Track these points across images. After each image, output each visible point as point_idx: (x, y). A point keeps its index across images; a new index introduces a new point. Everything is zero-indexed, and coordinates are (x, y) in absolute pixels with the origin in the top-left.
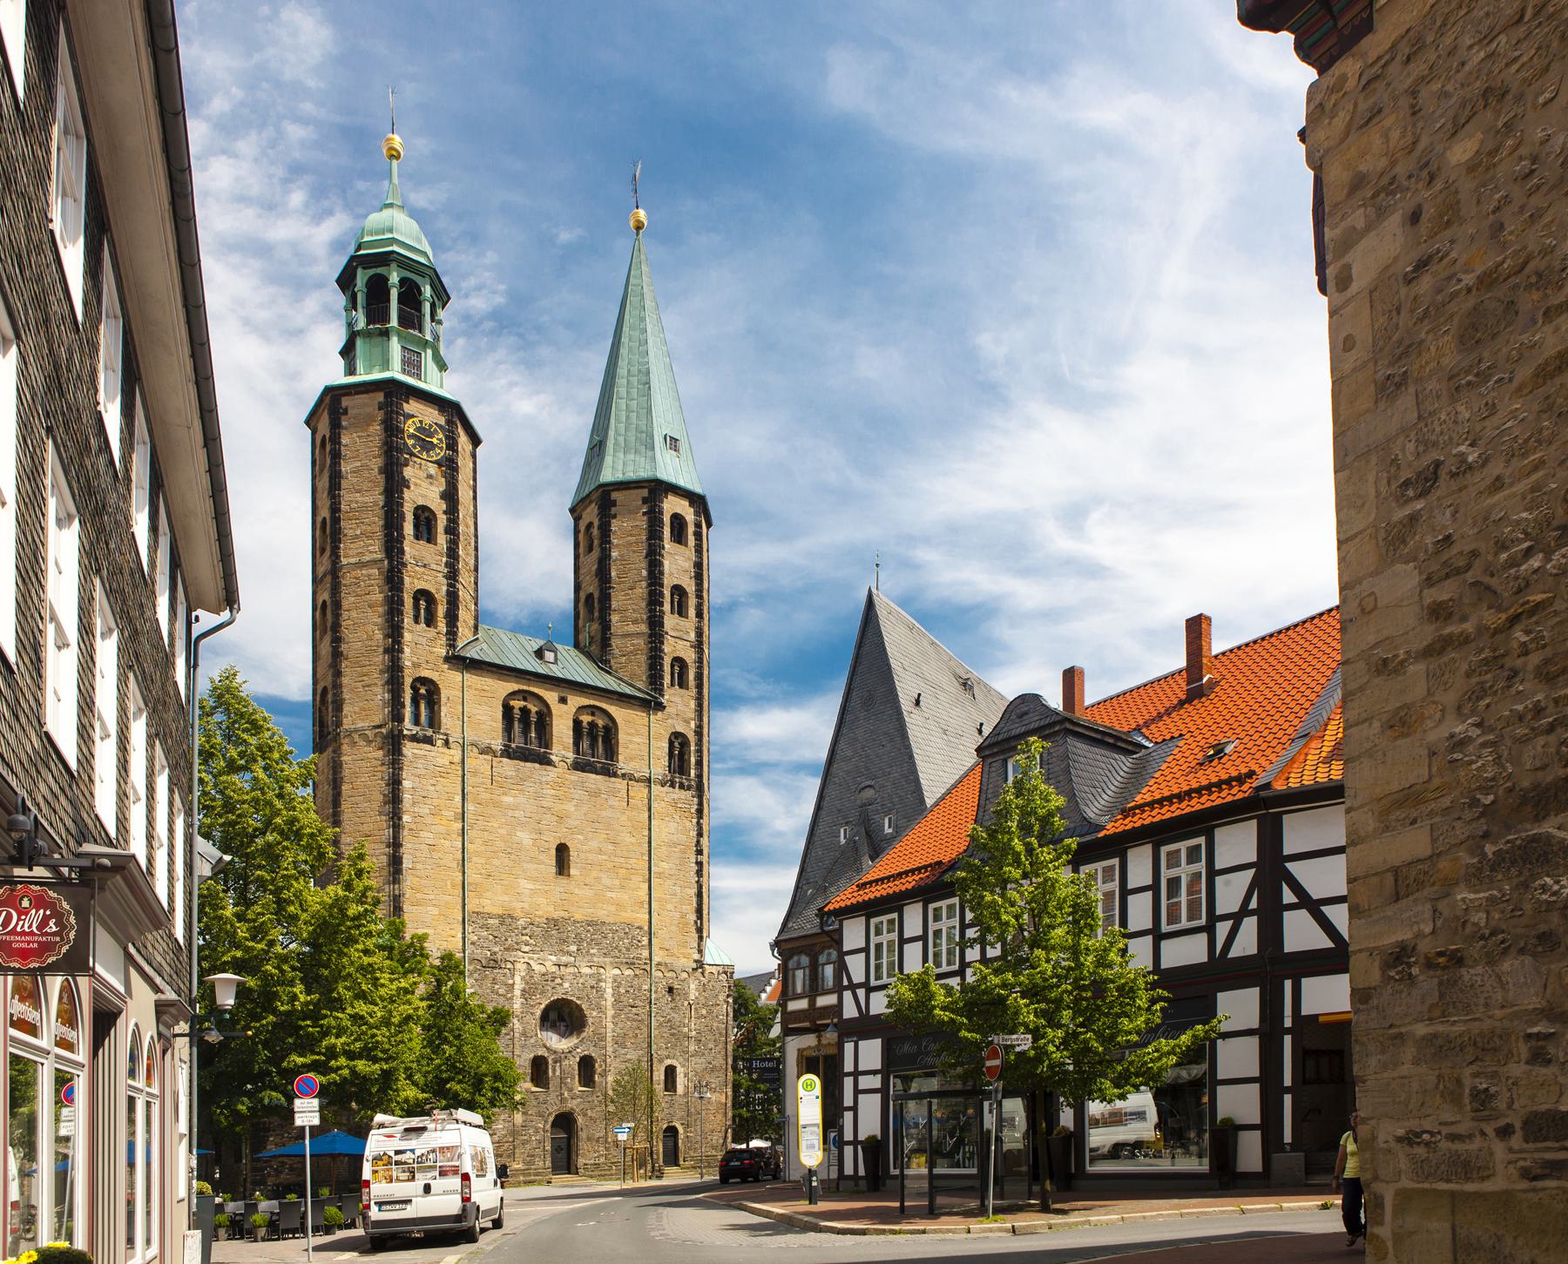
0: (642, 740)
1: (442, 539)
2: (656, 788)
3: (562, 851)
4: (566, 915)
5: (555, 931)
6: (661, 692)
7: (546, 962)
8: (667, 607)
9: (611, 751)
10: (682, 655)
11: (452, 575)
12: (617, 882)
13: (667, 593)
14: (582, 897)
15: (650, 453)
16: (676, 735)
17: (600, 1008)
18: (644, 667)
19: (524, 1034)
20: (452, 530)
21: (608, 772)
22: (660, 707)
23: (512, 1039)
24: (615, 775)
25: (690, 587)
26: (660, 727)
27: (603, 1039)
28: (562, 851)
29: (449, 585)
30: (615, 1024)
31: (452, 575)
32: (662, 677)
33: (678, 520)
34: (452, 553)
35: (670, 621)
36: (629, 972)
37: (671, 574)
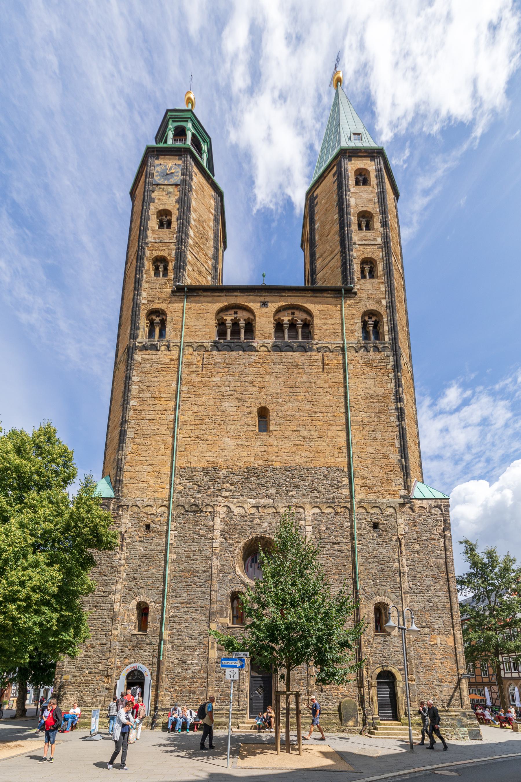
3: (263, 414)
5: (253, 478)
14: (282, 448)
16: (370, 313)
19: (222, 571)
22: (350, 293)
23: (210, 576)
26: (352, 311)
28: (263, 414)
37: (357, 205)
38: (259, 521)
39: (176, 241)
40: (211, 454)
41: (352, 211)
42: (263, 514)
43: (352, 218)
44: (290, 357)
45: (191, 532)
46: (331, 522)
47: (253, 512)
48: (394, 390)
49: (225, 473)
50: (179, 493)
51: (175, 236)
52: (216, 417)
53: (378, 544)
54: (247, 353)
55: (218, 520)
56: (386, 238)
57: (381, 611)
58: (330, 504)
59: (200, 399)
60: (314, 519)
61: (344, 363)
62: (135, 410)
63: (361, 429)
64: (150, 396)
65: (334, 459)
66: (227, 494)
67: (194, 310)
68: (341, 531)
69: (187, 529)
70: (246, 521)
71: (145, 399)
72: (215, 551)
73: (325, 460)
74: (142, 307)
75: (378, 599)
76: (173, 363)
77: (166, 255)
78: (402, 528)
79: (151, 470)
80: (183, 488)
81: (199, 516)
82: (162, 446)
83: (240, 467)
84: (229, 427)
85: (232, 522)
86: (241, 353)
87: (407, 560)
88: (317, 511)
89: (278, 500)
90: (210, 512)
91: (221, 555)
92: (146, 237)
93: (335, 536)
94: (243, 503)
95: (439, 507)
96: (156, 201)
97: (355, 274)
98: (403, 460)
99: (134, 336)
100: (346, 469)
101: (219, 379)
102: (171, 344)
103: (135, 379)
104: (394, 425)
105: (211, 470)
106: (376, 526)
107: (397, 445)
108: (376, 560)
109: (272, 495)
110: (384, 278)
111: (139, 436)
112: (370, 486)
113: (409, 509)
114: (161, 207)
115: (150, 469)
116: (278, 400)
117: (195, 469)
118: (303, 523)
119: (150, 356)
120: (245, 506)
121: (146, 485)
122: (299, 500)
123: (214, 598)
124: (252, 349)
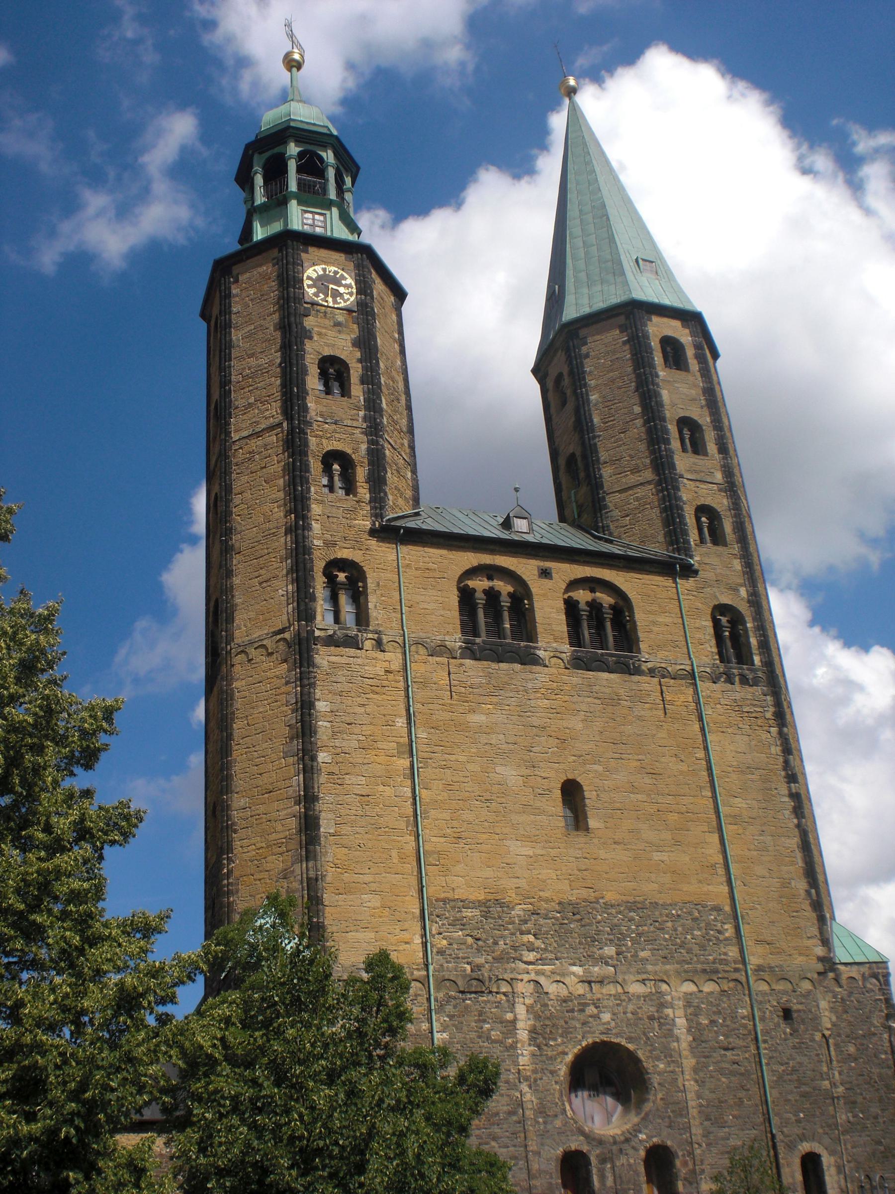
0: (669, 618)
1: (357, 391)
2: (705, 687)
4: (592, 895)
5: (575, 925)
6: (687, 550)
7: (568, 980)
8: (675, 444)
9: (627, 638)
10: (708, 501)
11: (374, 429)
12: (667, 835)
13: (672, 428)
15: (619, 279)
17: (669, 1055)
18: (658, 523)
19: (541, 1110)
20: (370, 378)
21: (628, 668)
23: (522, 1121)
24: (638, 671)
25: (704, 419)
27: (682, 1110)
29: (371, 442)
30: (700, 1083)
31: (374, 429)
32: (685, 533)
33: (671, 346)
34: (372, 405)
35: (683, 462)
36: (709, 987)
37: (674, 405)
38: (595, 1011)
39: (365, 426)
40: (488, 873)
41: (668, 414)
42: (599, 996)
43: (670, 427)
44: (605, 683)
45: (473, 1035)
46: (715, 1009)
47: (581, 992)
48: (781, 759)
49: (521, 913)
50: (441, 952)
51: (362, 413)
52: (487, 795)
53: (794, 1047)
54: (527, 667)
55: (521, 1010)
56: (729, 472)
57: (811, 1165)
58: (710, 974)
59: (453, 758)
60: (688, 1004)
61: (698, 703)
62: (329, 774)
63: (740, 831)
64: (355, 744)
65: (706, 888)
66: (531, 956)
67: (416, 569)
68: (734, 1026)
69: (465, 1028)
70: (572, 1011)
71: (346, 750)
72: (523, 1073)
73: (692, 889)
74: (316, 554)
75: (806, 1147)
76: (391, 676)
77: (349, 451)
78: (827, 1019)
79: (378, 904)
80: (445, 942)
81: (486, 1002)
82: (394, 853)
83: (547, 900)
84: (515, 818)
85: (547, 1013)
86: (517, 667)
87: (840, 1074)
88: (689, 987)
89: (624, 968)
90: (504, 994)
91: (535, 1080)
92: (306, 409)
93: (726, 1036)
94: (563, 975)
95: (875, 976)
96: (315, 338)
97: (691, 534)
98: (813, 891)
99: (305, 614)
100: (727, 908)
101: (483, 718)
102: (385, 639)
103: (321, 706)
104: (791, 825)
105: (492, 907)
106: (787, 1014)
107: (801, 863)
108: (795, 1077)
109: (611, 958)
110: (736, 548)
111: (346, 829)
112: (769, 939)
113: (833, 982)
114: (327, 352)
115: (375, 901)
116: (596, 767)
117: (466, 904)
118: (669, 1011)
119: (344, 660)
120: (567, 980)
121: (372, 935)
122: (657, 968)
123: (535, 1166)
124: (535, 661)
